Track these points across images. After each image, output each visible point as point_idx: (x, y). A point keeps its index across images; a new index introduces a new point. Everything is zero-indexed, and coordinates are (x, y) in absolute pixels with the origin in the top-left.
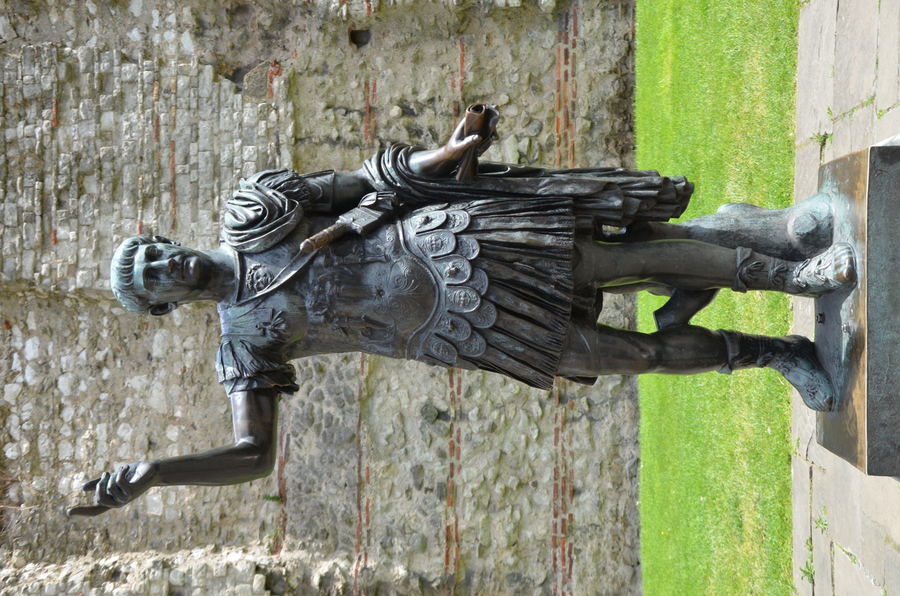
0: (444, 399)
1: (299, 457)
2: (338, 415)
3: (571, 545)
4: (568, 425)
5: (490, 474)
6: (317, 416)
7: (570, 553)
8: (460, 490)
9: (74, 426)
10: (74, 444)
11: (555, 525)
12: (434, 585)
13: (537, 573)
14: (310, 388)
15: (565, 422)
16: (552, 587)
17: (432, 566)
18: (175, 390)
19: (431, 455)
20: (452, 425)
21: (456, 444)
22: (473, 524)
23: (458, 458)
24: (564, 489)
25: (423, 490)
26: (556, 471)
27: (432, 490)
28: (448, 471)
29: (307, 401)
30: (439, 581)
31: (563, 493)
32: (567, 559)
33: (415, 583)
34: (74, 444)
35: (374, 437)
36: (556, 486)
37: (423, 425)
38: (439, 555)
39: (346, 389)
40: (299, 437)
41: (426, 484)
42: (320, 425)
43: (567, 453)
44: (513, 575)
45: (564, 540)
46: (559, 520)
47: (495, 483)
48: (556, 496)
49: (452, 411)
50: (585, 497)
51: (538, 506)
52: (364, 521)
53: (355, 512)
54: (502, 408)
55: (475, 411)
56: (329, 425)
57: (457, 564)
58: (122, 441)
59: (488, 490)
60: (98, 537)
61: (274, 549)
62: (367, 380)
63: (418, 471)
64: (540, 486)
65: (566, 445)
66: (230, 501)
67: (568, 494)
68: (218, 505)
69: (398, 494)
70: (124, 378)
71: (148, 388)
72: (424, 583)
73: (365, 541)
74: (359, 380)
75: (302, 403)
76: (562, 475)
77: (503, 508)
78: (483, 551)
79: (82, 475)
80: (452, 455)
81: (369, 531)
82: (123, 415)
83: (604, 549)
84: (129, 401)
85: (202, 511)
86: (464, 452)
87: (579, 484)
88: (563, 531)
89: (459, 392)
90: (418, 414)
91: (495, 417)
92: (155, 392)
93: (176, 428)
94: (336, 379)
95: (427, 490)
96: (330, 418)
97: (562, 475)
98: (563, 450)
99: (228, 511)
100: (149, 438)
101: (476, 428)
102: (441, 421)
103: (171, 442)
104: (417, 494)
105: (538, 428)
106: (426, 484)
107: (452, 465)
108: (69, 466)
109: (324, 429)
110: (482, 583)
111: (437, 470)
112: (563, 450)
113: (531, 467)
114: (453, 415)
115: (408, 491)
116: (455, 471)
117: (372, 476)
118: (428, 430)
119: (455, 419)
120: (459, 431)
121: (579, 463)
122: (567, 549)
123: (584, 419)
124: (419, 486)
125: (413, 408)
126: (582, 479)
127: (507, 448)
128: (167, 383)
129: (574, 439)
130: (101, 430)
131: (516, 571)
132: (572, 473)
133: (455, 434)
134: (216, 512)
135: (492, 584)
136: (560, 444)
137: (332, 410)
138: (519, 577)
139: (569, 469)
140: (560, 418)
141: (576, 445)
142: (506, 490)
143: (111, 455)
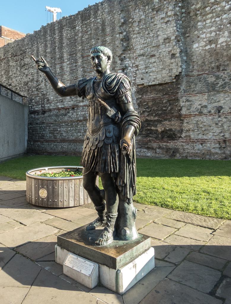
0: (223, 112)
1: (208, 78)
2: (219, 85)
3: (189, 143)
4: (218, 142)
5: (205, 124)
6: (218, 80)
7: (188, 143)
8: (201, 117)
9: (214, 21)
10: (210, 23)
11: (194, 139)
12: (179, 113)
13: (183, 135)
14: (226, 78)
15: (218, 141)
16: (180, 139)
17: (184, 112)
18: (224, 44)
19: (209, 109)
20: (217, 114)
21: (212, 115)
22: (193, 121)
23: (209, 116)
24: (202, 141)
25: (201, 108)
26: (207, 139)
27: (201, 110)
28: (205, 114)
29: (222, 77)
30: (180, 113)
31: (201, 141)
32: (186, 142)
33: (179, 108)
34: (210, 23)
35: (213, 95)
36: (203, 139)
37: (216, 107)
38: (186, 113)
39: (225, 87)
40: (213, 77)
41: (202, 109)
42: (216, 82)
43: (211, 142)
44: (183, 130)
45: (190, 141)
46: (195, 140)
47: (203, 125)
48: (200, 139)
49: (220, 114)
50: (201, 146)
51: (198, 135)
52: (193, 95)
53: (195, 93)
54: (222, 126)
55: (221, 120)
56: (216, 83)
57: (184, 117)
58: (211, 34)
59: (201, 123)
60: (188, 35)
61: (187, 76)
62: (227, 92)
63: (206, 107)
64: (203, 136)
65: (213, 142)
66: (197, 63)
67: (200, 142)
68: (196, 60)
69: (200, 102)
70: (227, 30)
71: (225, 37)
72: (180, 110)
73: (188, 96)
74: (228, 90)
75: (222, 76)
76: (206, 141)
77: (197, 127)
78: (187, 123)
79: (202, 27)
80: (210, 114)
81: (191, 96)
82: (218, 32)
83: (189, 150)
84: (221, 33)
85: (195, 57)
86: (210, 117)
87: (203, 145)
88: (192, 141)
89: (225, 115)
90: (219, 105)
91: (219, 125)
92: (224, 39)
93: (215, 46)
94: (228, 84)
95: (201, 109)
96: (218, 83)
97: (206, 141)
98: (212, 141)
99: (195, 63)
100: (211, 40)
101: (216, 120)
102: (218, 111)
103: (211, 46)
104: (199, 107)
105: (217, 135)
106: (202, 109)
107: (207, 115)
108: (204, 23)
109: (215, 82)
110: (181, 123)
111: (205, 111)
112: (212, 141)
113: (207, 134)
114: (219, 114)
115: (200, 105)
116: (206, 115)
117: (204, 96)
118: (215, 108)
119: (218, 114)
120: (216, 116)
121: (208, 145)
122: (188, 142)
123: (220, 146)
124: (202, 107)
125: (221, 104)
126: (205, 146)
127: (212, 128)
128: (226, 42)
129: (215, 144)
130: (213, 28)
131: (184, 131)
132: (207, 143)
133: (215, 115)
134: (194, 60)
135: (180, 125)
136: (213, 140)
137: (220, 84)
138: (183, 131)
139: (207, 142)
140: (220, 140)
141: (213, 144)
142: (202, 127)
143: (207, 32)
